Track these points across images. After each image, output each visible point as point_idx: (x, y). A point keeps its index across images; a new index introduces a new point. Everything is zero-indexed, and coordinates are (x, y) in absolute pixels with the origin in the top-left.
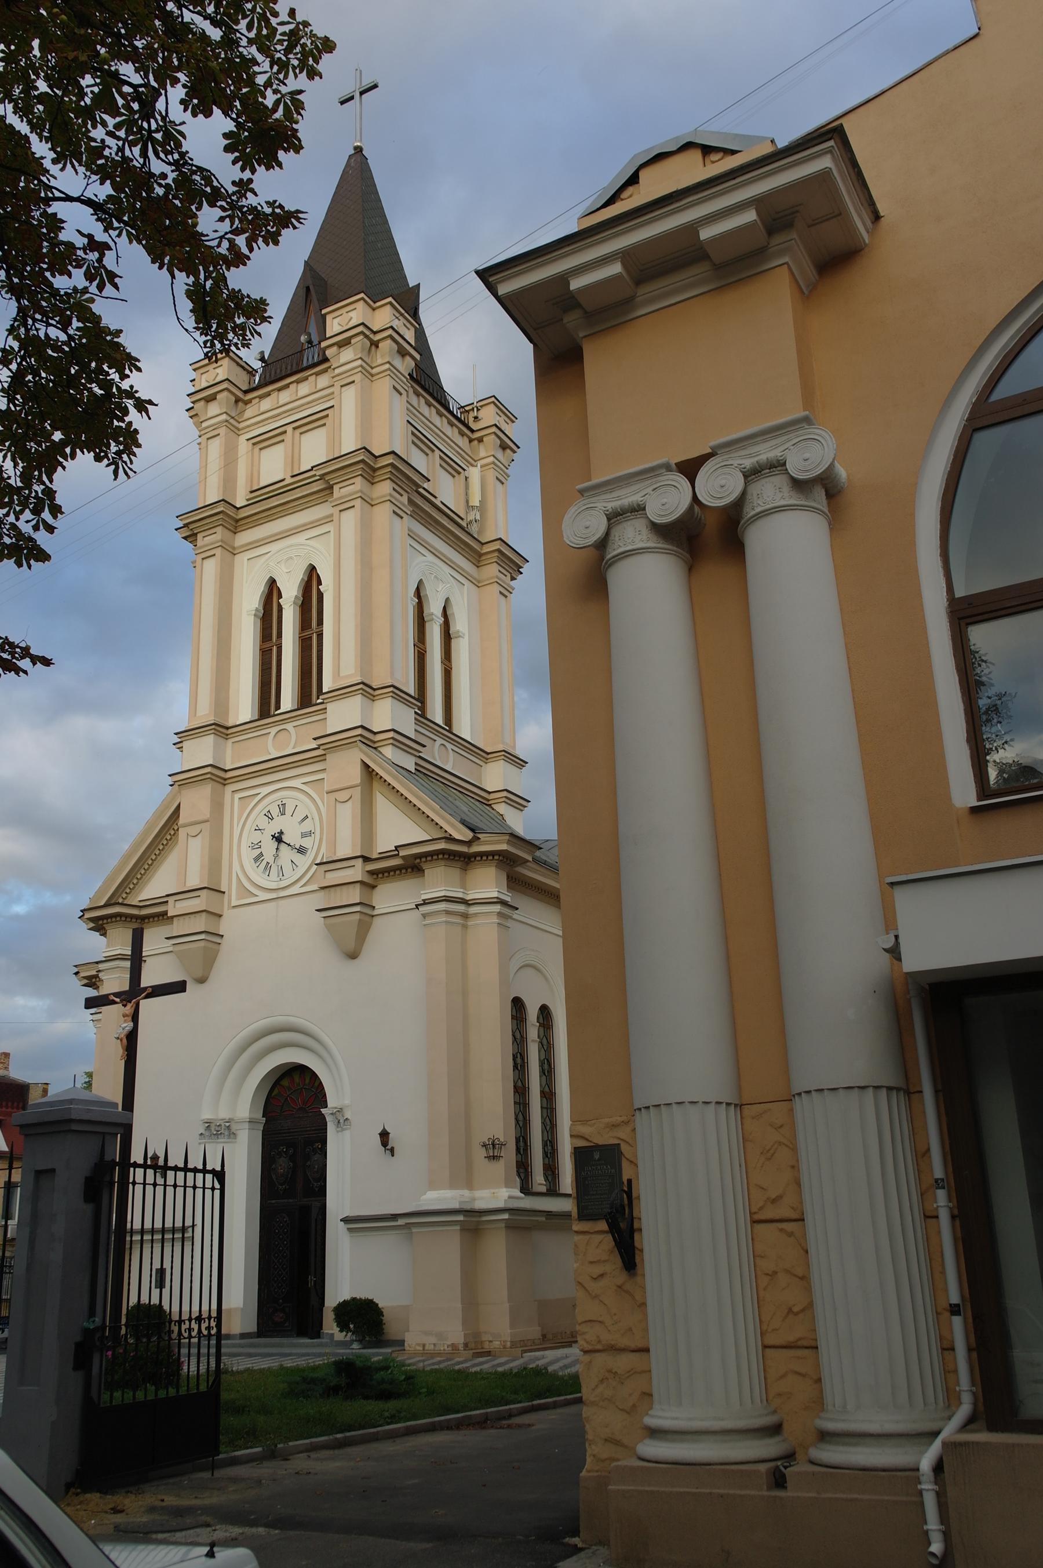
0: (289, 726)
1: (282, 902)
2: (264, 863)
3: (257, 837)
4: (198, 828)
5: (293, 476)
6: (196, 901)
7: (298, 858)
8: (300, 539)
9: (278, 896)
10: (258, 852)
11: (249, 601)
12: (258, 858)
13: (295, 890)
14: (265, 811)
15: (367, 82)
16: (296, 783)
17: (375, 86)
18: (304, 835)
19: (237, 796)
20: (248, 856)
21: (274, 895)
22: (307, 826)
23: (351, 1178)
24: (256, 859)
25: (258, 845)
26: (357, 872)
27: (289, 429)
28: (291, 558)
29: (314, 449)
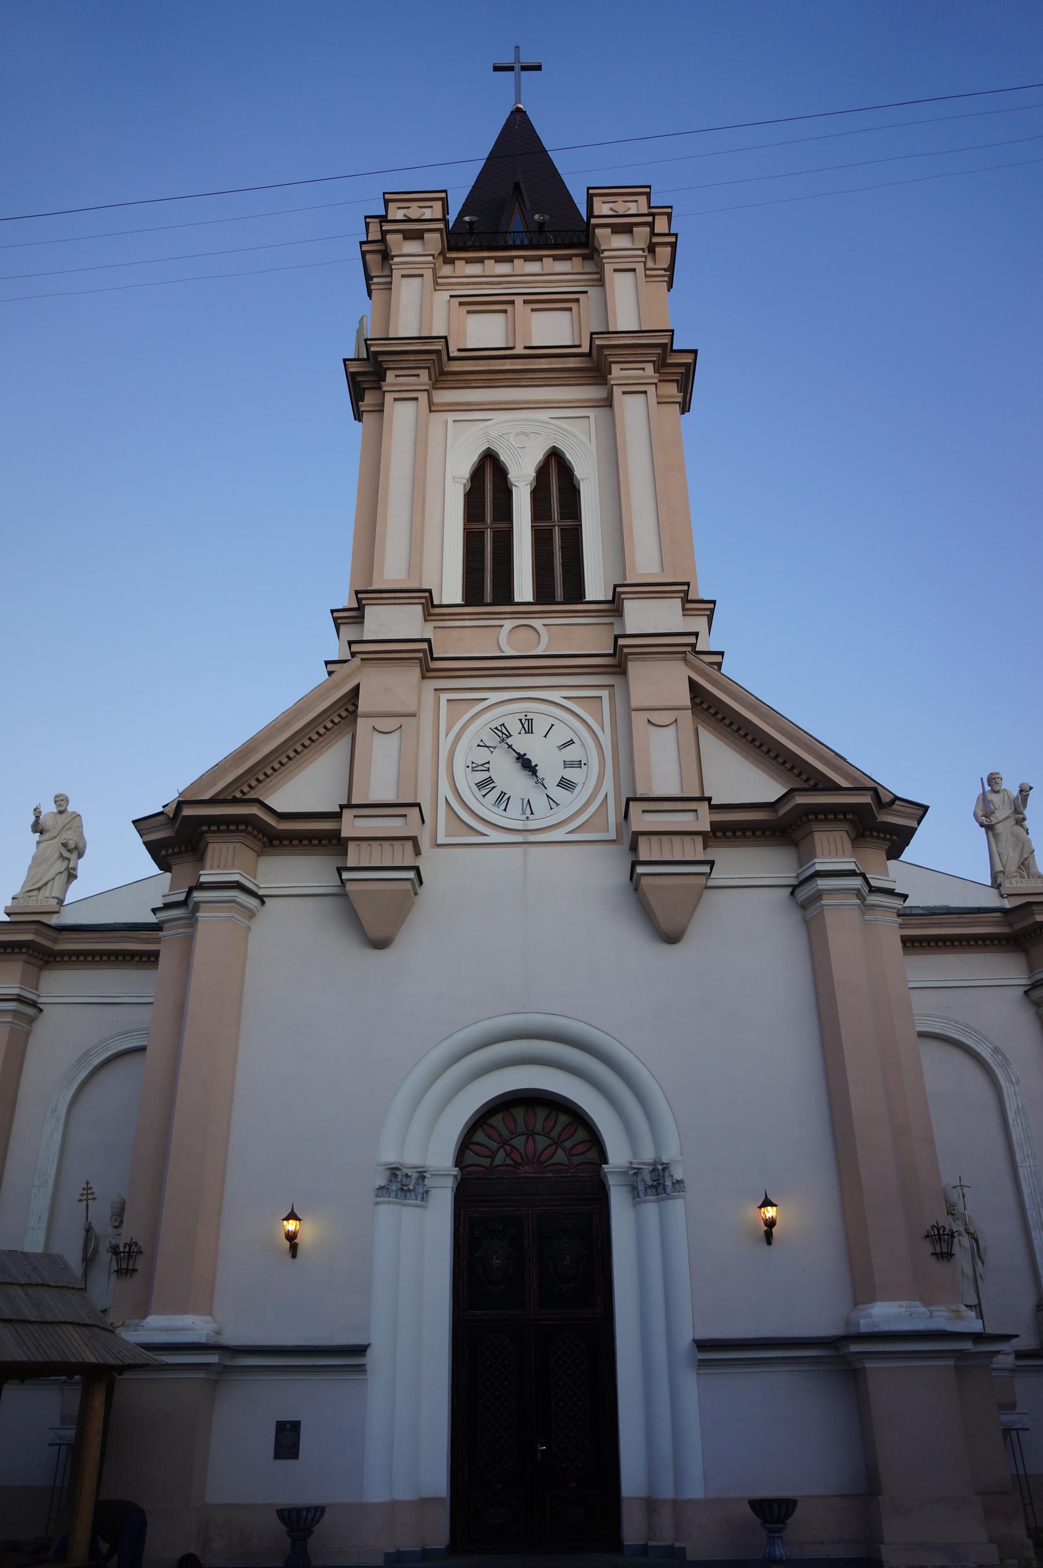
0: (537, 623)
1: (533, 850)
2: (495, 794)
3: (482, 756)
4: (394, 723)
5: (526, 348)
6: (398, 822)
7: (558, 794)
8: (545, 415)
9: (525, 840)
10: (484, 775)
11: (460, 467)
12: (486, 784)
13: (558, 835)
15: (527, 59)
16: (555, 696)
17: (538, 68)
18: (568, 764)
19: (444, 697)
21: (519, 838)
22: (572, 753)
23: (664, 1281)
24: (480, 785)
25: (486, 766)
26: (704, 821)
27: (519, 300)
28: (525, 434)
29: (551, 329)
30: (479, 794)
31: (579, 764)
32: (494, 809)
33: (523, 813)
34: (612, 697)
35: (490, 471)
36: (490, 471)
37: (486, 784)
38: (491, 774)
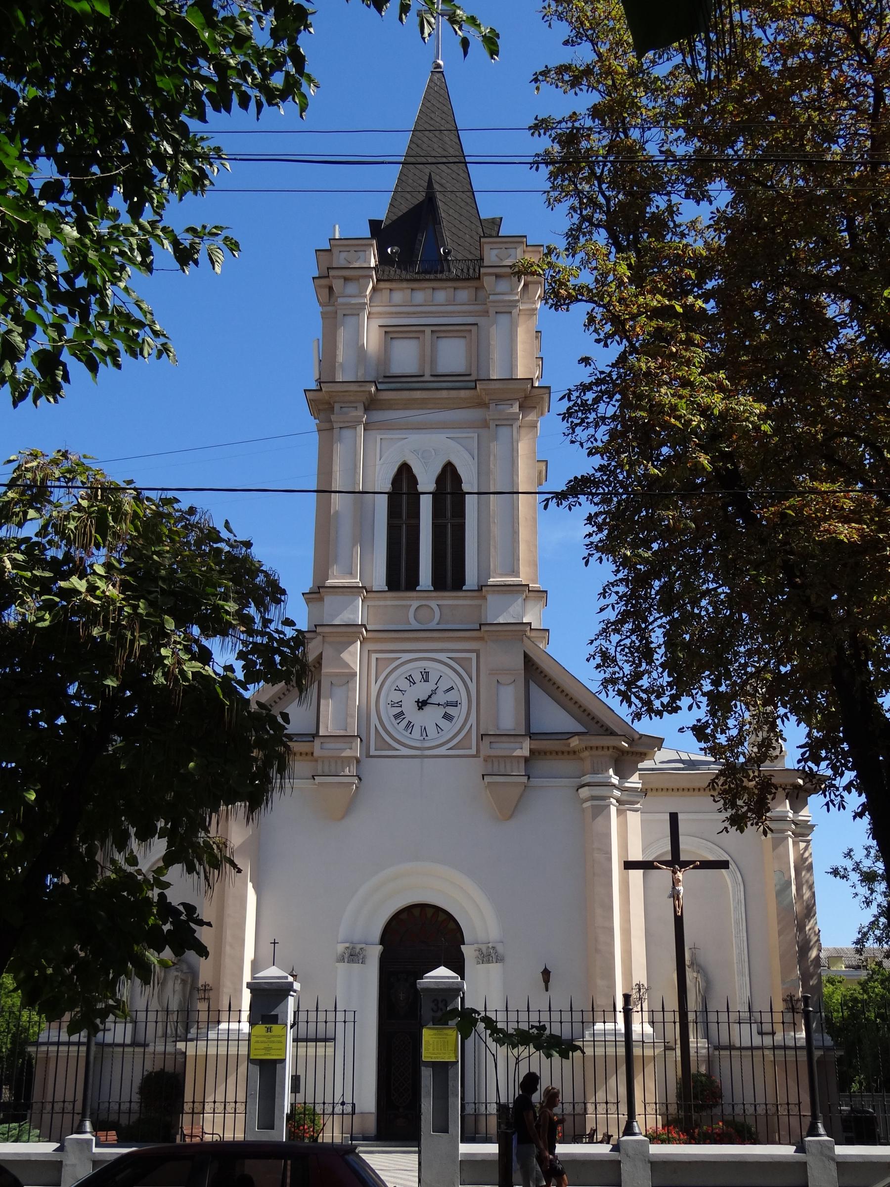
0: (433, 604)
10: (398, 710)
12: (399, 716)
13: (442, 751)
14: (407, 675)
16: (442, 656)
20: (388, 713)
24: (396, 716)
25: (399, 704)
30: (395, 722)
31: (455, 704)
32: (404, 733)
33: (422, 735)
34: (478, 657)
35: (404, 476)
36: (404, 476)
37: (399, 716)
38: (402, 709)
